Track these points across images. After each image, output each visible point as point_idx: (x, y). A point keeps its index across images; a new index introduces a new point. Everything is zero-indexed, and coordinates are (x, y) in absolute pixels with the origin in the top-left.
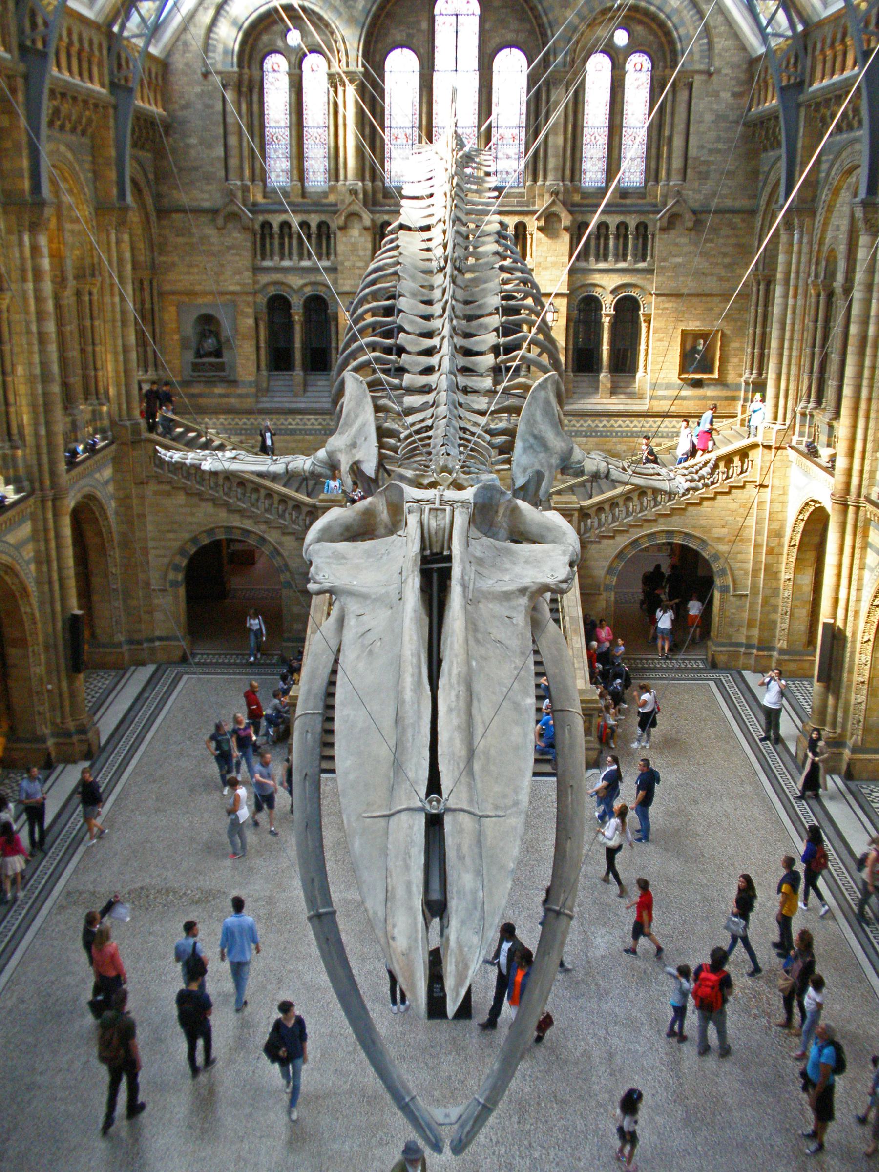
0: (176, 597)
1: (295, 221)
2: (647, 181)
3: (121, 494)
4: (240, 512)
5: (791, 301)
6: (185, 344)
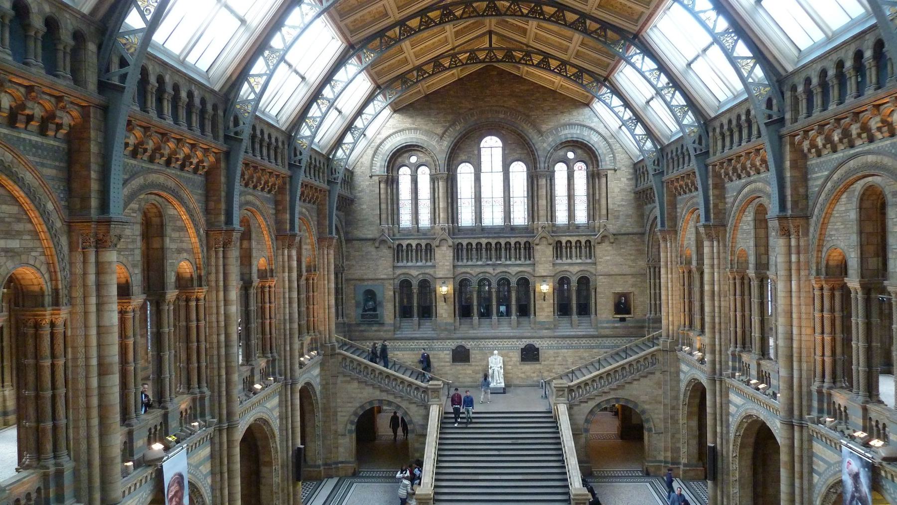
0: (351, 438)
2: (588, 221)
3: (324, 382)
4: (387, 391)
5: (670, 276)
6: (357, 305)
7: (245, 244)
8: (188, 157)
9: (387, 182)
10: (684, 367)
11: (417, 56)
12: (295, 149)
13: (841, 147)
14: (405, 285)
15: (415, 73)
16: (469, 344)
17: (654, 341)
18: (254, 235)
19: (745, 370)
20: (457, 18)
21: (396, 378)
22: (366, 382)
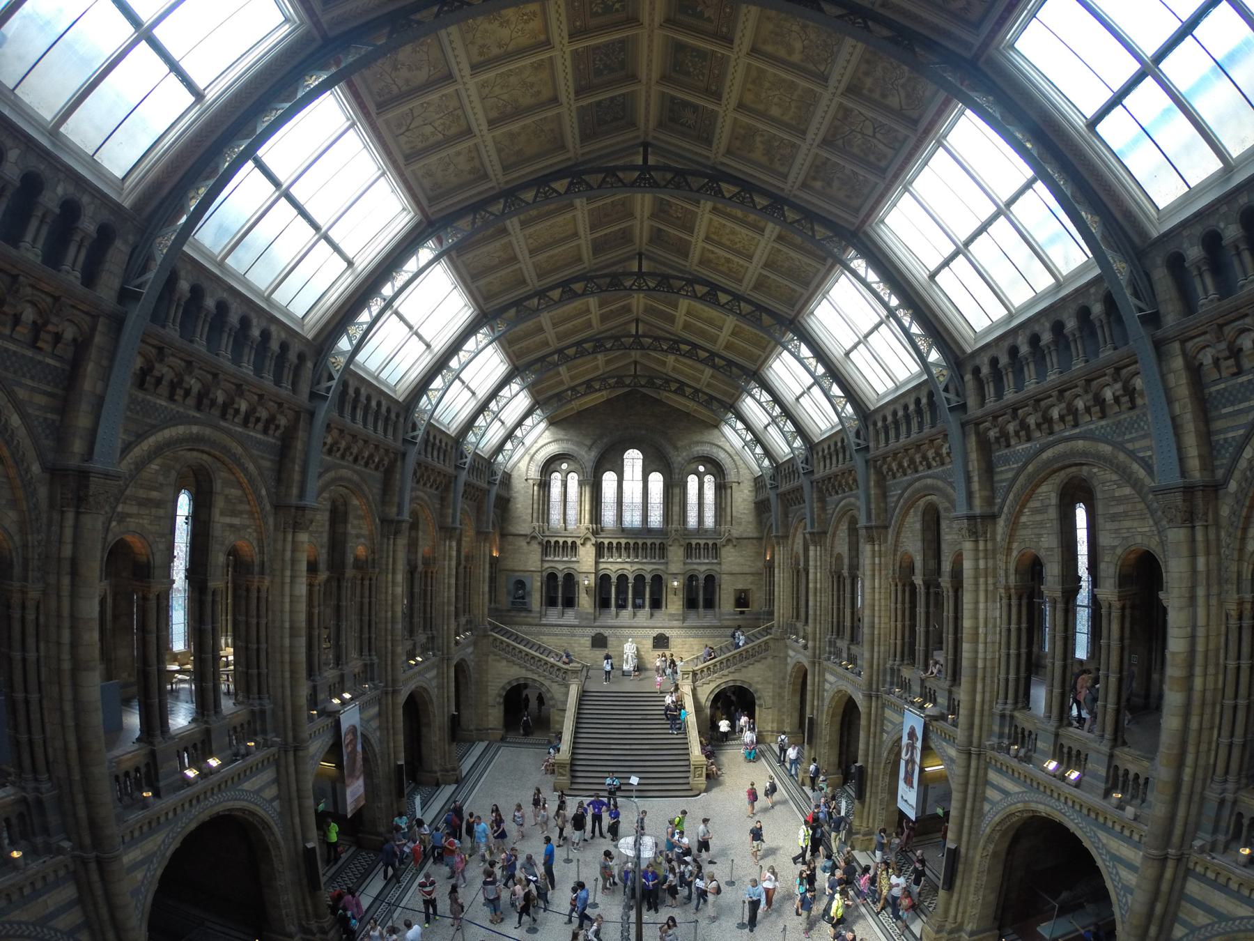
1: (561, 540)
2: (716, 525)
6: (509, 593)
7: (413, 533)
8: (371, 456)
9: (540, 485)
10: (791, 653)
11: (572, 378)
12: (462, 453)
13: (909, 471)
14: (552, 577)
15: (569, 392)
16: (606, 632)
17: (767, 631)
18: (421, 526)
19: (838, 654)
20: (607, 350)
21: (540, 660)
22: (513, 662)
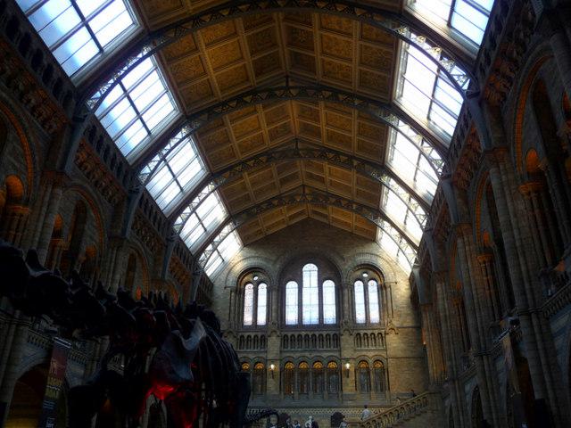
1: (253, 335)
18: (137, 269)
